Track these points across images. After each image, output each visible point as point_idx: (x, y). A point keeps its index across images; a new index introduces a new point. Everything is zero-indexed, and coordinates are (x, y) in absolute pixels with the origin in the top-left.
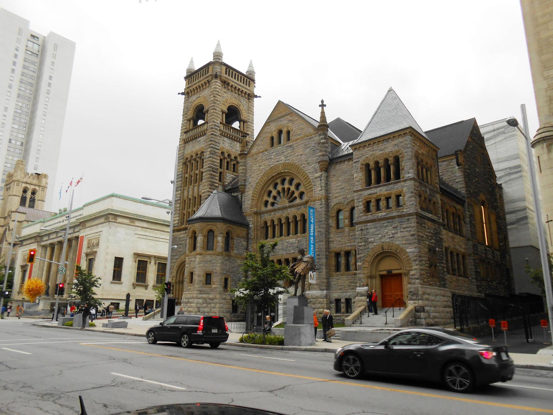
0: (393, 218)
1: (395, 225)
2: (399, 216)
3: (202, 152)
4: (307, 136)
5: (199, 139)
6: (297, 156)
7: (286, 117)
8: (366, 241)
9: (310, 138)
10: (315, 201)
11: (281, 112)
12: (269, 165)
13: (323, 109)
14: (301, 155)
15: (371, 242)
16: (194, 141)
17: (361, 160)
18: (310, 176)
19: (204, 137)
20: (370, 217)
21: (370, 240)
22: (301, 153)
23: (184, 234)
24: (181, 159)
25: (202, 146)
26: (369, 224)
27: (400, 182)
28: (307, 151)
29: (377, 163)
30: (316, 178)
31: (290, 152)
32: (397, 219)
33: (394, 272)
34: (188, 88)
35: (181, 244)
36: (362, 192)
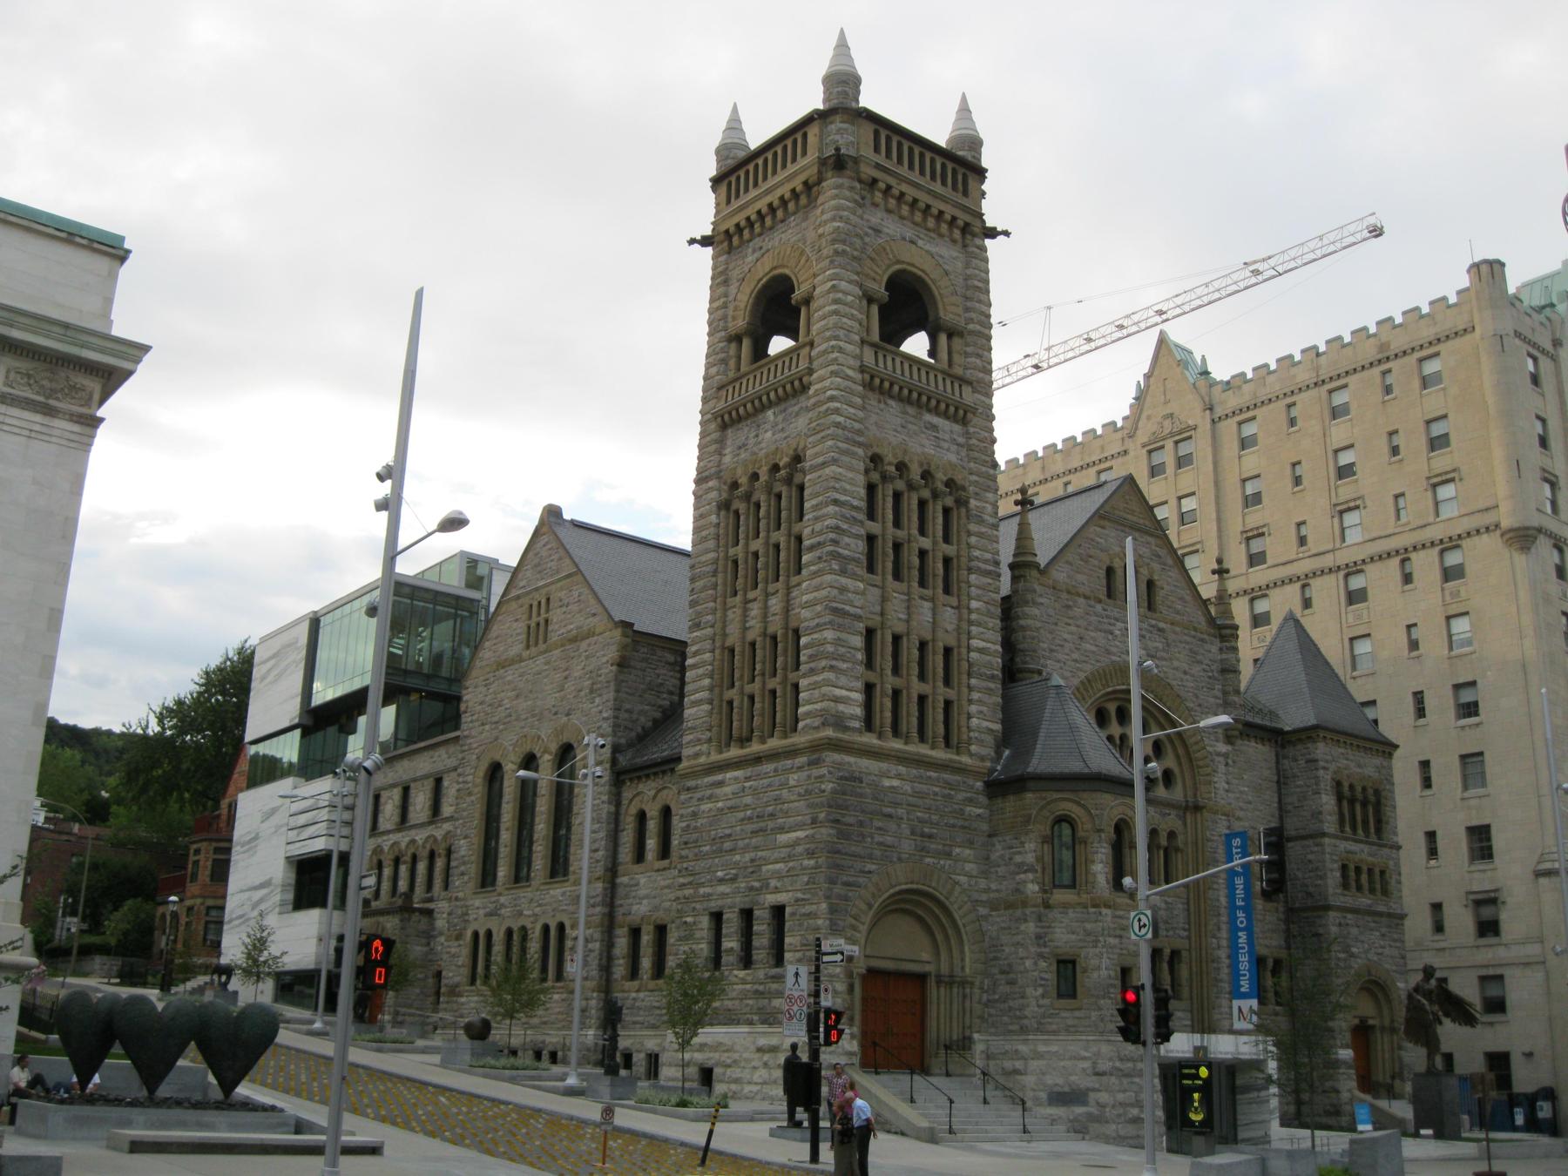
0: (1381, 914)
1: (1384, 930)
2: (1389, 915)
3: (950, 483)
4: (1195, 629)
5: (928, 417)
6: (1176, 669)
7: (1150, 539)
8: (1346, 949)
9: (1202, 640)
10: (1216, 813)
11: (1132, 512)
12: (1108, 652)
13: (1221, 579)
14: (1185, 673)
15: (1352, 955)
16: (911, 410)
17: (1333, 767)
18: (1207, 741)
19: (957, 428)
20: (1348, 900)
21: (1354, 950)
22: (1186, 667)
23: (899, 776)
24: (860, 444)
25: (953, 458)
26: (1349, 916)
27: (1385, 846)
28: (1196, 669)
29: (1351, 787)
30: (1219, 754)
31: (1160, 646)
32: (1384, 919)
33: (1371, 1022)
34: (878, 166)
35: (890, 816)
36: (1337, 842)
